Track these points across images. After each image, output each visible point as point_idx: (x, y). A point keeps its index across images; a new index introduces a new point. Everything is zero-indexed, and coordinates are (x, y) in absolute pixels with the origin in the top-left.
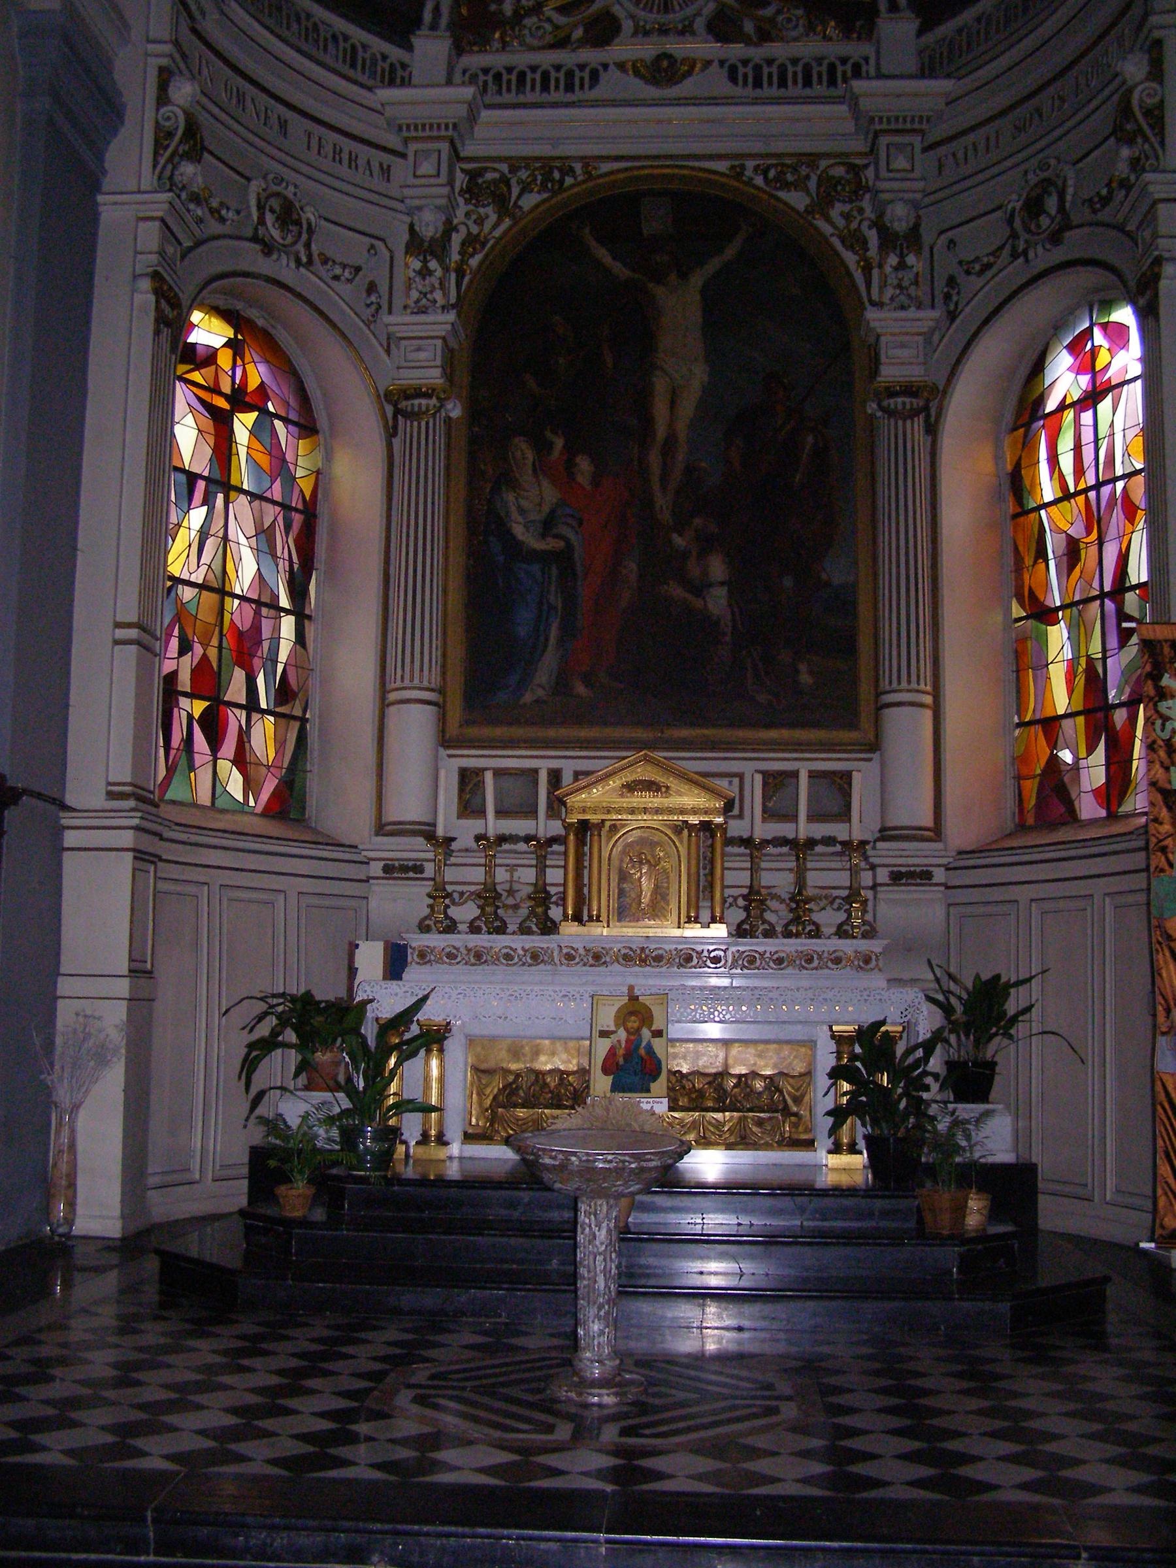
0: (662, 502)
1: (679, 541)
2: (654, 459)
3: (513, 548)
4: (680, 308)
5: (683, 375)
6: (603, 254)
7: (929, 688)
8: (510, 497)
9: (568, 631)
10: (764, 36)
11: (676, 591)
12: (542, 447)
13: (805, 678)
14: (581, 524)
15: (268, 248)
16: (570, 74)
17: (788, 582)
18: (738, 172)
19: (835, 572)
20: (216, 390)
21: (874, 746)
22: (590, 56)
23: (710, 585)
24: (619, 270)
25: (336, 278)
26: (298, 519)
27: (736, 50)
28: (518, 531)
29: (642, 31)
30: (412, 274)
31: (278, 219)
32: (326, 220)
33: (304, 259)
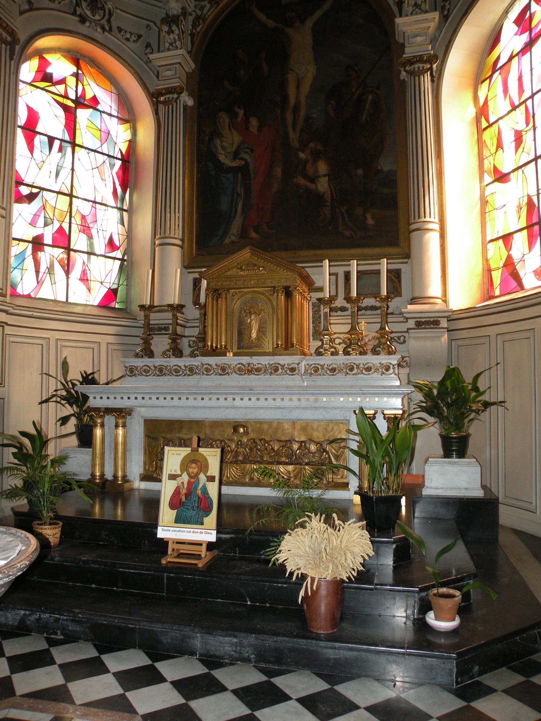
0: (293, 136)
1: (302, 155)
2: (289, 116)
3: (219, 165)
5: (303, 71)
6: (262, 17)
7: (437, 220)
8: (218, 142)
9: (246, 207)
11: (302, 181)
12: (233, 115)
13: (370, 221)
14: (252, 151)
15: (83, 20)
17: (360, 172)
19: (385, 164)
20: (66, 96)
21: (408, 256)
23: (319, 177)
24: (271, 24)
25: (128, 40)
26: (118, 163)
28: (222, 158)
30: (164, 34)
31: (88, 5)
32: (121, 10)
33: (107, 28)
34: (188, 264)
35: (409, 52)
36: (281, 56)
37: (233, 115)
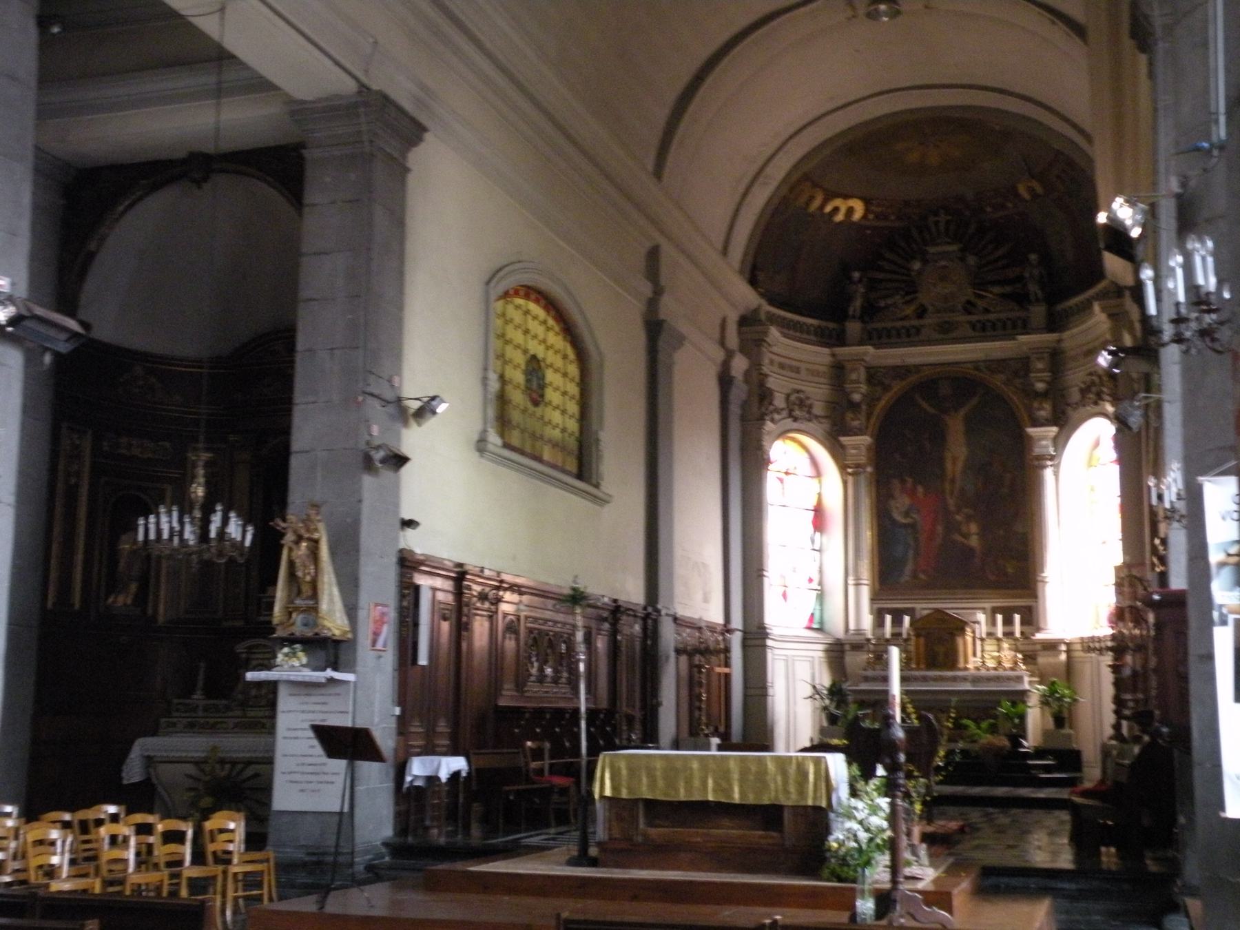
0: (951, 502)
1: (958, 518)
3: (894, 522)
4: (956, 426)
5: (957, 451)
6: (925, 405)
9: (917, 554)
10: (987, 311)
11: (959, 538)
12: (903, 481)
15: (796, 419)
16: (908, 330)
18: (977, 369)
19: (1019, 528)
22: (916, 322)
24: (931, 410)
27: (974, 318)
29: (938, 311)
34: (874, 599)
35: (1037, 451)
36: (939, 437)
37: (903, 481)
